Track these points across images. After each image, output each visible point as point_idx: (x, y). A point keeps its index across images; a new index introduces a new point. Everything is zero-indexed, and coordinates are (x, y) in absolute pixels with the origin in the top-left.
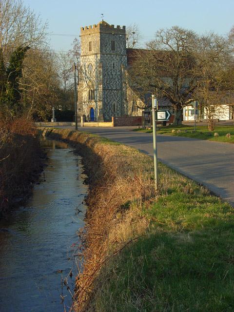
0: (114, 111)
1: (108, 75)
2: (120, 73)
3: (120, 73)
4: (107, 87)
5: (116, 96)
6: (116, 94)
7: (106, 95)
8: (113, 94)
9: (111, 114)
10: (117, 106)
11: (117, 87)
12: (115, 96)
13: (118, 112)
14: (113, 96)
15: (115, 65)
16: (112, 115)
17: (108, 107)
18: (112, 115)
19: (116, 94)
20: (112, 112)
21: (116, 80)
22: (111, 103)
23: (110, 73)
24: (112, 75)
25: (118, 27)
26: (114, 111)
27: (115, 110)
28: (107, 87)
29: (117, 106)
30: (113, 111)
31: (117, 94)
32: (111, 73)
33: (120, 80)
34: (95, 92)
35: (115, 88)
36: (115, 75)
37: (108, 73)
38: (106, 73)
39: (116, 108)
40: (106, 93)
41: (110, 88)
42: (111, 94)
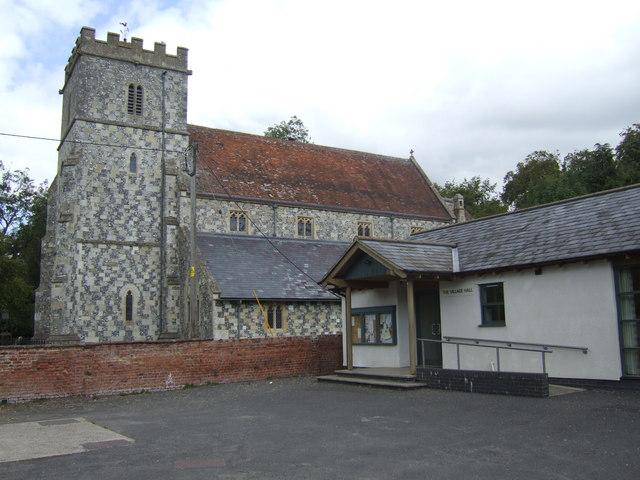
0: (129, 317)
1: (108, 190)
2: (156, 189)
3: (156, 189)
4: (97, 232)
5: (140, 268)
6: (137, 259)
8: (123, 257)
10: (142, 301)
12: (133, 264)
13: (145, 322)
14: (126, 265)
15: (139, 162)
17: (101, 303)
19: (137, 259)
20: (117, 324)
23: (113, 186)
24: (126, 193)
25: (160, 47)
26: (129, 317)
27: (135, 317)
28: (97, 232)
29: (142, 301)
30: (122, 318)
31: (143, 259)
32: (121, 186)
33: (156, 214)
35: (133, 239)
36: (139, 193)
37: (105, 184)
38: (96, 184)
39: (135, 306)
41: (111, 237)
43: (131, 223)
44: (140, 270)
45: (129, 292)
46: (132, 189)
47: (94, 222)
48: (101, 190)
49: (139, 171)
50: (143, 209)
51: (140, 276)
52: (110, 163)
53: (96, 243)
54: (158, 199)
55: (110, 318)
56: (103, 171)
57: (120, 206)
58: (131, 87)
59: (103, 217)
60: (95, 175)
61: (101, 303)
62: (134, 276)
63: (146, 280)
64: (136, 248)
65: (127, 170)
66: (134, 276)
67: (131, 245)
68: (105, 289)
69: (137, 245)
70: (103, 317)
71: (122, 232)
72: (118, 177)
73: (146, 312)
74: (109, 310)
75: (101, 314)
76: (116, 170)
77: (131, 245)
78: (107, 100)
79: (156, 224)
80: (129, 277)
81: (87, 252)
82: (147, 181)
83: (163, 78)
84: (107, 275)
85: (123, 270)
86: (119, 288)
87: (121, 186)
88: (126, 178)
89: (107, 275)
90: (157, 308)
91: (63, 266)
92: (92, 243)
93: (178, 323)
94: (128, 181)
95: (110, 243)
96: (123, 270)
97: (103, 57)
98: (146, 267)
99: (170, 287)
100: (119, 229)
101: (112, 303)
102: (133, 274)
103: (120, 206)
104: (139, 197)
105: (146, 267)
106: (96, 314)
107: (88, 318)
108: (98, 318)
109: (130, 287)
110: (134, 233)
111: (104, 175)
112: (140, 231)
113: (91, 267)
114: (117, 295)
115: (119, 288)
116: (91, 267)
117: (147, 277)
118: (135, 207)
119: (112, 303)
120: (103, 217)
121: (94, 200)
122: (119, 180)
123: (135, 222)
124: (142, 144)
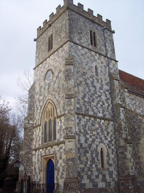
0: (103, 166)
1: (87, 84)
2: (108, 88)
3: (108, 88)
4: (84, 109)
5: (105, 133)
6: (104, 127)
7: (85, 126)
8: (97, 126)
9: (96, 173)
10: (108, 155)
11: (106, 113)
12: (102, 131)
13: (112, 169)
14: (99, 131)
15: (99, 71)
16: (97, 177)
17: (88, 155)
18: (97, 177)
19: (104, 127)
20: (98, 170)
21: (103, 98)
22: (94, 146)
23: (89, 82)
24: (95, 87)
25: (100, 17)
26: (103, 166)
27: (106, 166)
28: (84, 109)
29: (108, 155)
30: (100, 166)
31: (107, 128)
32: (92, 82)
33: (110, 101)
34: (58, 120)
35: (100, 115)
36: (101, 88)
37: (85, 80)
38: (81, 79)
39: (105, 158)
40: (82, 123)
41: (91, 113)
42: (93, 125)
43: (99, 105)
44: (106, 135)
45: (102, 149)
46: (98, 86)
47: (82, 102)
48: (83, 83)
49: (100, 76)
50: (103, 98)
51: (106, 139)
52: (86, 69)
53: (84, 115)
54: (110, 93)
55: (94, 166)
56: (84, 72)
57: (93, 94)
58: (91, 32)
59: (86, 100)
60: (80, 74)
61: (88, 155)
62: (103, 139)
63: (109, 141)
64: (103, 121)
65: (94, 74)
66: (103, 139)
67: (101, 118)
68: (90, 146)
69: (103, 119)
70: (91, 165)
71: (96, 111)
72: (91, 77)
73: (111, 162)
74: (93, 161)
75: (89, 163)
76: (89, 74)
77: (101, 118)
78: (81, 35)
79: (110, 108)
80: (101, 139)
81: (80, 120)
82: (104, 82)
83: (103, 32)
84: (91, 137)
85: (98, 134)
86: (97, 146)
87: (92, 82)
88: (94, 78)
89: (91, 137)
90: (116, 160)
91: (71, 128)
92: (82, 115)
93: (134, 169)
94: (95, 81)
95: (90, 116)
96: (98, 134)
97: (78, 13)
98: (108, 133)
99: (128, 145)
100: (94, 108)
101: (94, 155)
102: (102, 136)
103: (93, 94)
104: (101, 91)
105: (108, 133)
106: (87, 163)
107: (82, 166)
108: (88, 166)
109: (102, 145)
110: (101, 111)
111: (85, 75)
112: (103, 111)
113: (82, 131)
114: (96, 150)
115: (97, 146)
116: (82, 131)
117: (109, 139)
118: (100, 96)
119: (94, 155)
120: (86, 100)
121: (81, 88)
122: (91, 79)
123: (101, 105)
124: (99, 61)
